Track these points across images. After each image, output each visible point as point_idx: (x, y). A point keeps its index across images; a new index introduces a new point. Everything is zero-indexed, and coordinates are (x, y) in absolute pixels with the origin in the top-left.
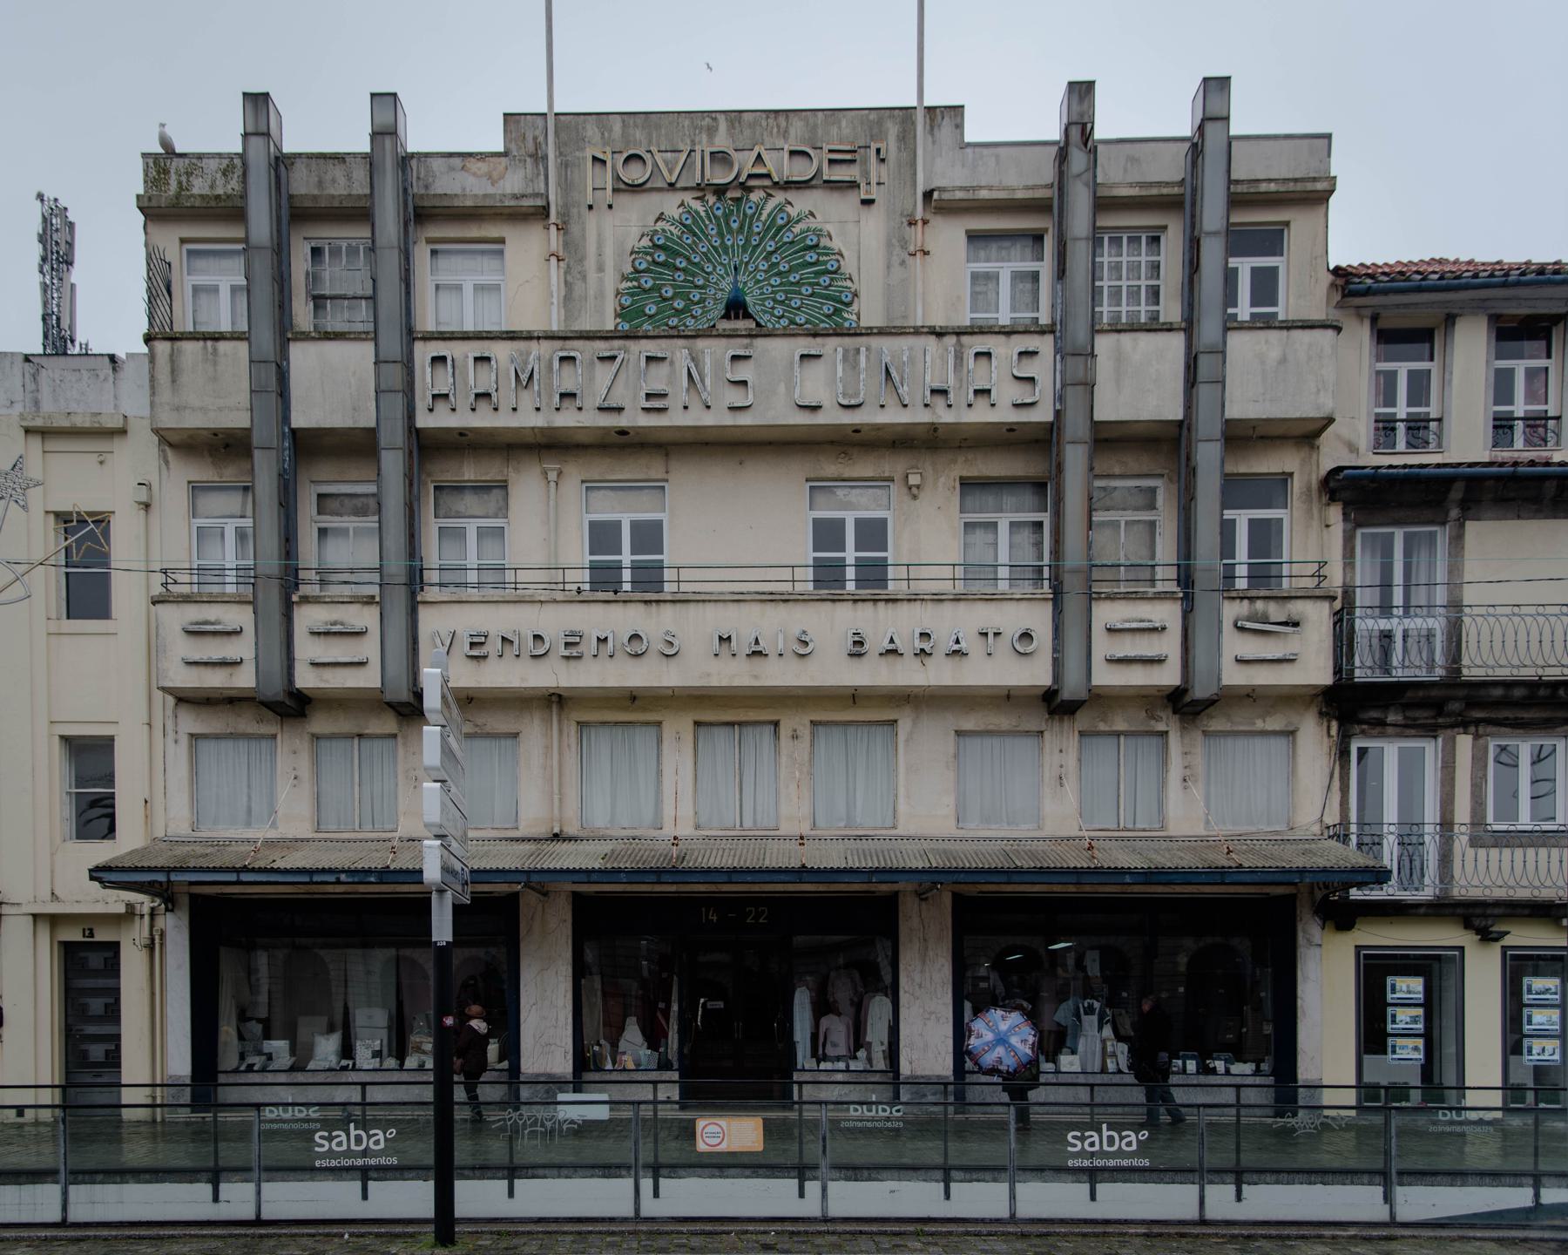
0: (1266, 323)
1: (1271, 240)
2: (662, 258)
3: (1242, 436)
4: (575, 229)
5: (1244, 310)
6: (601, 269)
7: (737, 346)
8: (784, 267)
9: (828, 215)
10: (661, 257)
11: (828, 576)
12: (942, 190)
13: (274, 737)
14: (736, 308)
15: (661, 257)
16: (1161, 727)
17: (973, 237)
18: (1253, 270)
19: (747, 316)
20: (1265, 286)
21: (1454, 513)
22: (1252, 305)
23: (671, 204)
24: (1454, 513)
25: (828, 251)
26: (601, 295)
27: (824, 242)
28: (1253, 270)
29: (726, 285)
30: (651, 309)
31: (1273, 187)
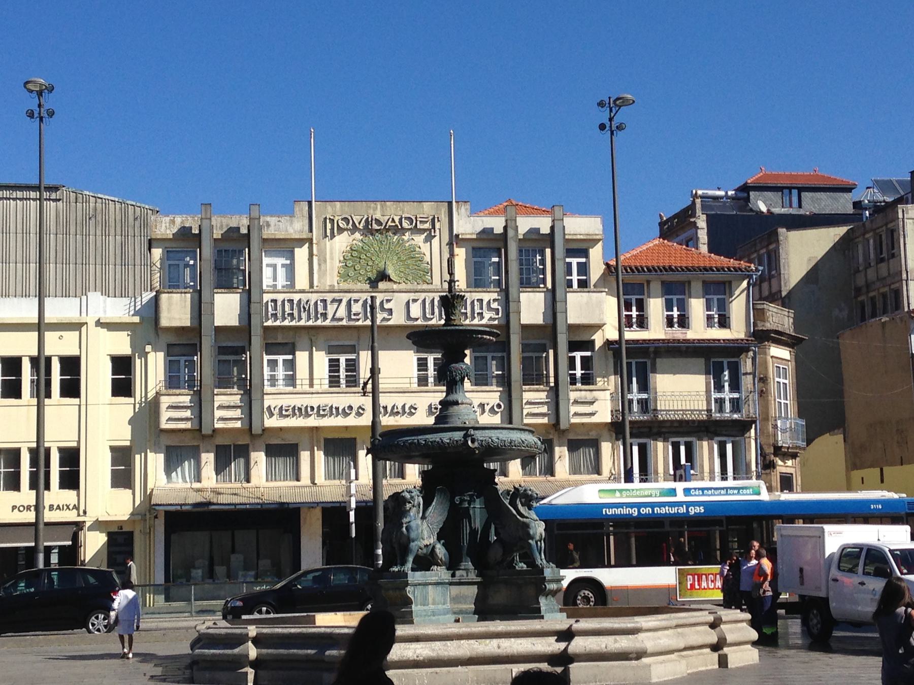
0: (583, 284)
1: (584, 253)
2: (353, 256)
3: (572, 328)
4: (322, 244)
5: (575, 278)
6: (332, 258)
7: (387, 296)
8: (403, 258)
9: (419, 239)
10: (355, 254)
11: (423, 381)
12: (462, 234)
13: (198, 446)
14: (383, 276)
15: (355, 254)
16: (551, 437)
17: (473, 248)
18: (578, 263)
19: (390, 280)
20: (583, 269)
21: (652, 356)
22: (578, 275)
23: (357, 235)
24: (652, 356)
25: (420, 253)
26: (332, 269)
27: (417, 249)
28: (578, 263)
29: (382, 265)
30: (352, 273)
31: (582, 237)
